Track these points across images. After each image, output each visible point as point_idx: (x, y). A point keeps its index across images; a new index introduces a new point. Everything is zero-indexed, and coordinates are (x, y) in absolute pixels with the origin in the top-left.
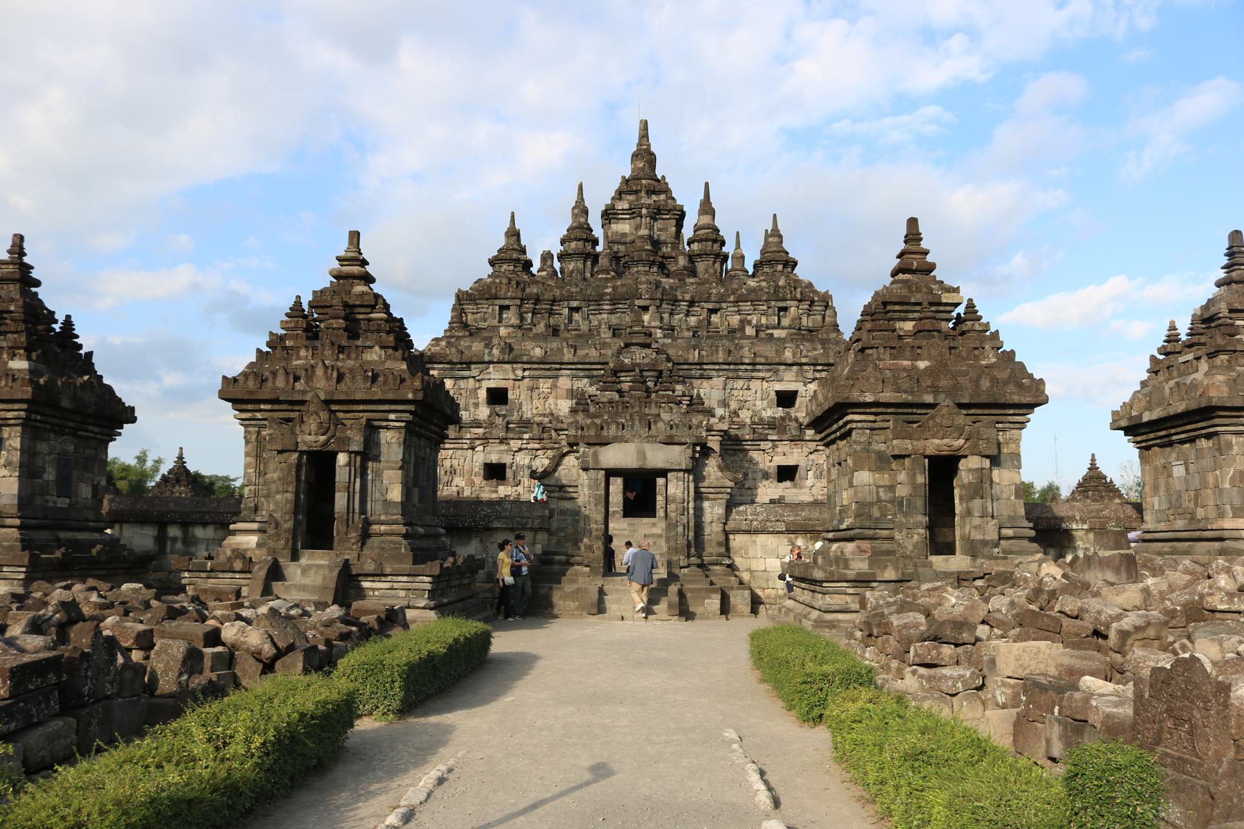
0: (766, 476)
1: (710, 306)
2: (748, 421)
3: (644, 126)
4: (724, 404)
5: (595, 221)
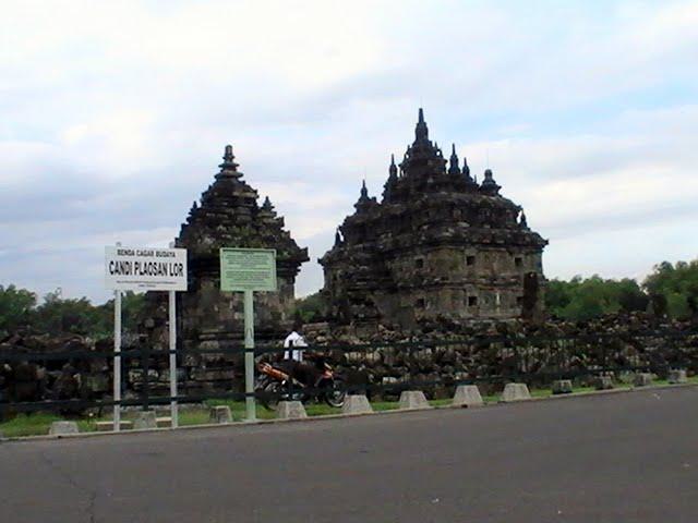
3: (421, 110)
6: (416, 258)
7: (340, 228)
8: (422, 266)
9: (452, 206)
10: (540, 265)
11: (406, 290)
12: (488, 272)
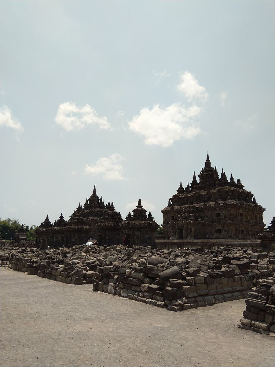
0: (215, 232)
3: (208, 155)
5: (198, 180)
7: (170, 199)
8: (220, 216)
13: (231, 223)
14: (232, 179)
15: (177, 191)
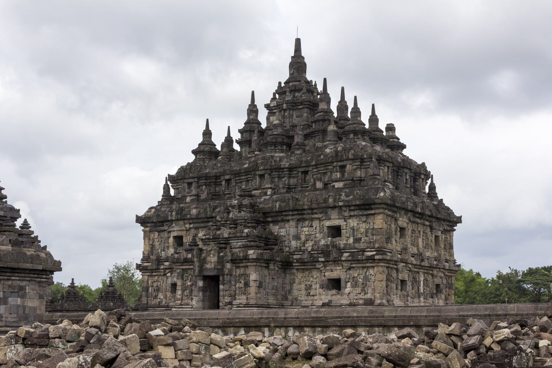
0: (322, 287)
1: (303, 170)
2: (310, 249)
3: (298, 42)
4: (297, 237)
5: (263, 117)
6: (328, 223)
7: (171, 178)
9: (380, 160)
10: (451, 247)
11: (309, 264)
12: (415, 250)
13: (377, 257)
14: (374, 119)
15: (194, 152)
